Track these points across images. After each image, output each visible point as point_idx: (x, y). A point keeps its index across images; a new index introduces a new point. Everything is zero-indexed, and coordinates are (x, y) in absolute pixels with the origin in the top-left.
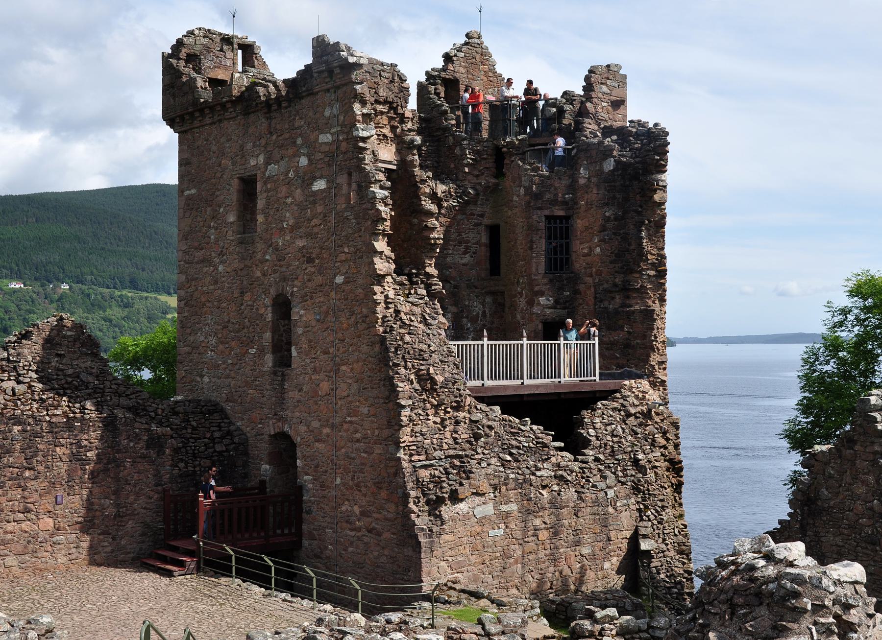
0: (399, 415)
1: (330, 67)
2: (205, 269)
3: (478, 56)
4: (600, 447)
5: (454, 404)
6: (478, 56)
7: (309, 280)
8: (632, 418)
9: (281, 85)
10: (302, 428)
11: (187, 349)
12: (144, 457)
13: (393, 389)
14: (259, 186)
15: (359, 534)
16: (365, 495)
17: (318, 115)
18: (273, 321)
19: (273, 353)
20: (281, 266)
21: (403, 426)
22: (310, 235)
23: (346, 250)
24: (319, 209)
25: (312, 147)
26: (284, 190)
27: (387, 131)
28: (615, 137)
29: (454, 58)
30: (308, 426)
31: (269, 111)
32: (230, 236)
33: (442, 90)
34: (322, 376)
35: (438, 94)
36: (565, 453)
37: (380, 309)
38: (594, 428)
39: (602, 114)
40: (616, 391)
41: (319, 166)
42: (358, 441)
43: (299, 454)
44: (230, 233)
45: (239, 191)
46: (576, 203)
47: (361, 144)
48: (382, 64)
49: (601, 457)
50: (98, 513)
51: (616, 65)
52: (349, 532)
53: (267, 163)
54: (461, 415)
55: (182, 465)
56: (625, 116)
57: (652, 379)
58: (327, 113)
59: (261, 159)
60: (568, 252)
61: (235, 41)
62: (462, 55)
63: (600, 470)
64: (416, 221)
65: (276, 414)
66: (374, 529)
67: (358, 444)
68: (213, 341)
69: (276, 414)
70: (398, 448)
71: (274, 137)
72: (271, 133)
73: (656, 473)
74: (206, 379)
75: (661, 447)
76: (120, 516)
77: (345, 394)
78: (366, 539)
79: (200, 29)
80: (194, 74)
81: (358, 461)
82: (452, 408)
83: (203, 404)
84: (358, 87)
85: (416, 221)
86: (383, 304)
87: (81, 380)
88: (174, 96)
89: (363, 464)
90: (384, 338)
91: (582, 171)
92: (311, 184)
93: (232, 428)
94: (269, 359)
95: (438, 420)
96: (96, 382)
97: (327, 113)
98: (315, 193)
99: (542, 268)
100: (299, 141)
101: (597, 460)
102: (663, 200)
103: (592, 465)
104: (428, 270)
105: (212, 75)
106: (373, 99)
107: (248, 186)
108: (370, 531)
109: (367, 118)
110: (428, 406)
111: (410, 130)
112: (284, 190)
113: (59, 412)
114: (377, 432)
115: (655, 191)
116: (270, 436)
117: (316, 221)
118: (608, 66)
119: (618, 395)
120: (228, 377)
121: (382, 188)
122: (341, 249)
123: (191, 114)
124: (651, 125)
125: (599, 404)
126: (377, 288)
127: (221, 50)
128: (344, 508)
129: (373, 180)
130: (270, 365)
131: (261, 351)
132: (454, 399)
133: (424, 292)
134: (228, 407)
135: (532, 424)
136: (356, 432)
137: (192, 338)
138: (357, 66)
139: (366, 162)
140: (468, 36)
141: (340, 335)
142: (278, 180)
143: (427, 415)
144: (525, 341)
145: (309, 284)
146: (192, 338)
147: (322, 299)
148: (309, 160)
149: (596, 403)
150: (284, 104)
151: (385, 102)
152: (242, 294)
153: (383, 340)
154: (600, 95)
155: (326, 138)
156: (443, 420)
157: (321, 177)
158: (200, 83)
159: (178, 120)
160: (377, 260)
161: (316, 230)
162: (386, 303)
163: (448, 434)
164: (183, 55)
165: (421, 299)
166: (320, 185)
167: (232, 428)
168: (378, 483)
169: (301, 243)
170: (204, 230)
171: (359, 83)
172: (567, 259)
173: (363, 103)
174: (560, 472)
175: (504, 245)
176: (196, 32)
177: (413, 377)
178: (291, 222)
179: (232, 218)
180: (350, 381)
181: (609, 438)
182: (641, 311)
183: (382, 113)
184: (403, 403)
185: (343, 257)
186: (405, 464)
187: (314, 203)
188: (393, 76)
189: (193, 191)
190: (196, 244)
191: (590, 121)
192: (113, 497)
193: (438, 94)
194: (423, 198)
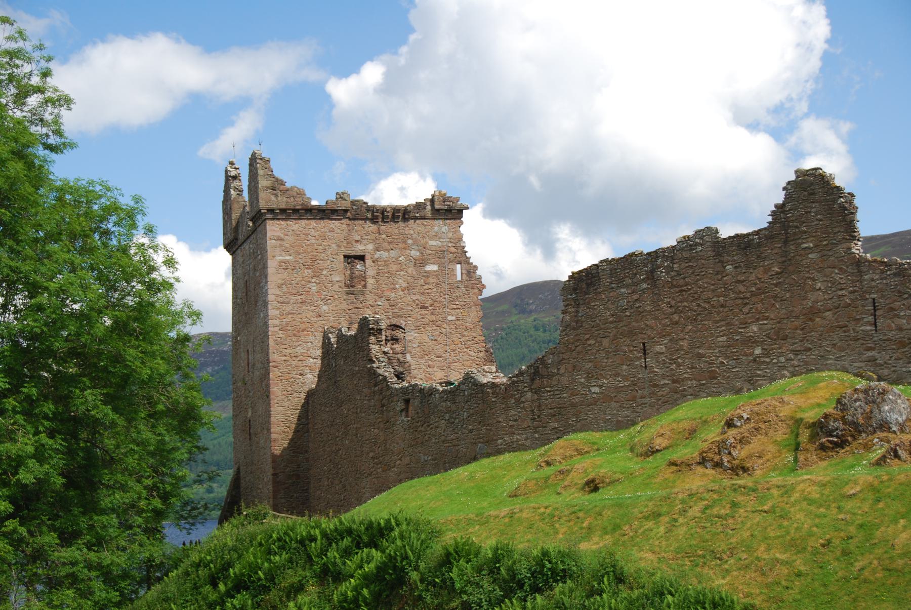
24: (431, 280)
32: (336, 288)
34: (435, 369)
58: (436, 229)
59: (370, 247)
71: (384, 236)
88: (276, 195)
97: (436, 229)
98: (426, 272)
100: (410, 242)
112: (394, 268)
123: (295, 211)
137: (288, 351)
141: (453, 347)
146: (288, 351)
157: (434, 264)
178: (405, 285)
185: (455, 307)
187: (428, 277)
189: (288, 258)
190: (294, 292)
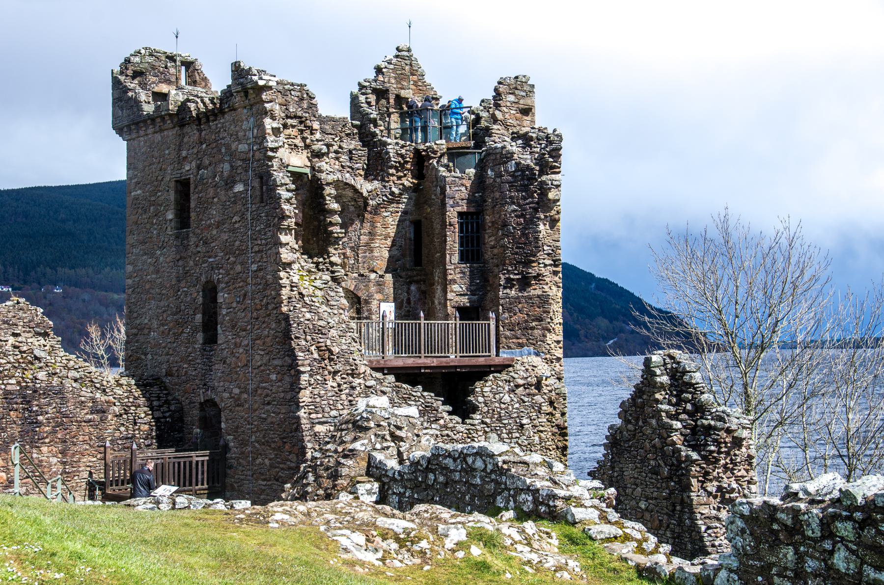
0: (299, 379)
1: (245, 88)
2: (150, 260)
3: (407, 68)
4: (488, 412)
5: (350, 372)
6: (407, 68)
7: (231, 269)
8: (521, 389)
9: (207, 100)
10: (226, 395)
11: (135, 331)
12: (90, 421)
13: (294, 357)
14: (192, 186)
15: (269, 483)
16: (274, 449)
17: (237, 128)
18: (203, 304)
19: (204, 332)
20: (210, 257)
21: (301, 389)
22: (233, 231)
23: (259, 242)
24: (238, 207)
25: (232, 154)
26: (211, 192)
27: (298, 142)
28: (520, 142)
29: (384, 70)
30: (231, 393)
31: (200, 124)
33: (372, 98)
35: (369, 103)
36: (453, 417)
37: (285, 292)
38: (484, 396)
39: (510, 121)
40: (510, 366)
41: (239, 172)
42: (269, 404)
43: (223, 419)
44: (169, 228)
45: (176, 192)
46: (485, 201)
47: (270, 154)
48: (292, 85)
49: (488, 421)
50: (46, 470)
51: (524, 76)
52: (261, 482)
53: (199, 168)
54: (357, 381)
55: (122, 429)
56: (533, 122)
57: (548, 356)
59: (194, 164)
60: (478, 245)
61: (178, 58)
62: (392, 67)
63: (486, 432)
64: (322, 218)
65: (205, 385)
66: (281, 477)
67: (269, 407)
68: (155, 324)
69: (205, 385)
70: (298, 408)
71: (204, 146)
72: (202, 144)
73: (540, 438)
74: (149, 357)
75: (548, 414)
76: (66, 473)
77: (259, 364)
78: (275, 487)
79: (146, 49)
80: (139, 90)
81: (269, 420)
82: (348, 374)
83: (145, 377)
84: (266, 105)
85: (322, 218)
86: (288, 288)
87: (35, 356)
89: (272, 423)
90: (288, 316)
91: (489, 172)
92: (233, 187)
93: (170, 398)
94: (200, 337)
95: (335, 385)
96: (49, 358)
99: (456, 258)
100: (223, 150)
101: (483, 422)
102: (557, 198)
103: (478, 427)
104: (333, 259)
105: (156, 89)
106: (283, 115)
107: (183, 187)
108: (277, 480)
109: (276, 132)
110: (326, 373)
111: (318, 140)
113: (13, 381)
114: (282, 395)
115: (550, 189)
116: (201, 403)
117: (236, 218)
118: (517, 77)
119: (511, 369)
120: (167, 354)
121: (288, 190)
122: (256, 242)
124: (550, 131)
125: (491, 377)
126: (282, 274)
127: (166, 67)
128: (258, 462)
129: (279, 183)
130: (201, 342)
131: (195, 330)
132: (348, 368)
133: (329, 278)
134: (167, 380)
135: (424, 390)
136: (267, 395)
138: (267, 88)
139: (275, 168)
140: (398, 49)
142: (207, 183)
143: (325, 380)
144: (423, 321)
145: (231, 272)
146: (138, 322)
147: (241, 284)
148: (232, 166)
149: (488, 375)
150: (211, 118)
151: (295, 117)
152: (179, 281)
153: (287, 318)
154: (509, 104)
155: (243, 147)
156: (339, 385)
157: (240, 181)
158: (143, 97)
159: (125, 130)
160: (283, 250)
161: (236, 226)
162: (292, 286)
163: (344, 397)
164: (130, 72)
165: (325, 284)
166: (239, 188)
167: (170, 398)
168: (284, 438)
169: (225, 237)
170: (148, 226)
171: (268, 102)
172: (478, 251)
173: (273, 118)
174: (446, 432)
175: (425, 239)
176: (143, 51)
177: (313, 348)
179: (170, 216)
180: (262, 353)
181: (497, 405)
182: (538, 296)
183: (293, 127)
184: (302, 369)
185: (256, 248)
186: (303, 421)
187: (235, 203)
188: (302, 94)
189: (139, 192)
191: (499, 127)
192: (60, 456)
193: (369, 103)
194: (328, 198)
